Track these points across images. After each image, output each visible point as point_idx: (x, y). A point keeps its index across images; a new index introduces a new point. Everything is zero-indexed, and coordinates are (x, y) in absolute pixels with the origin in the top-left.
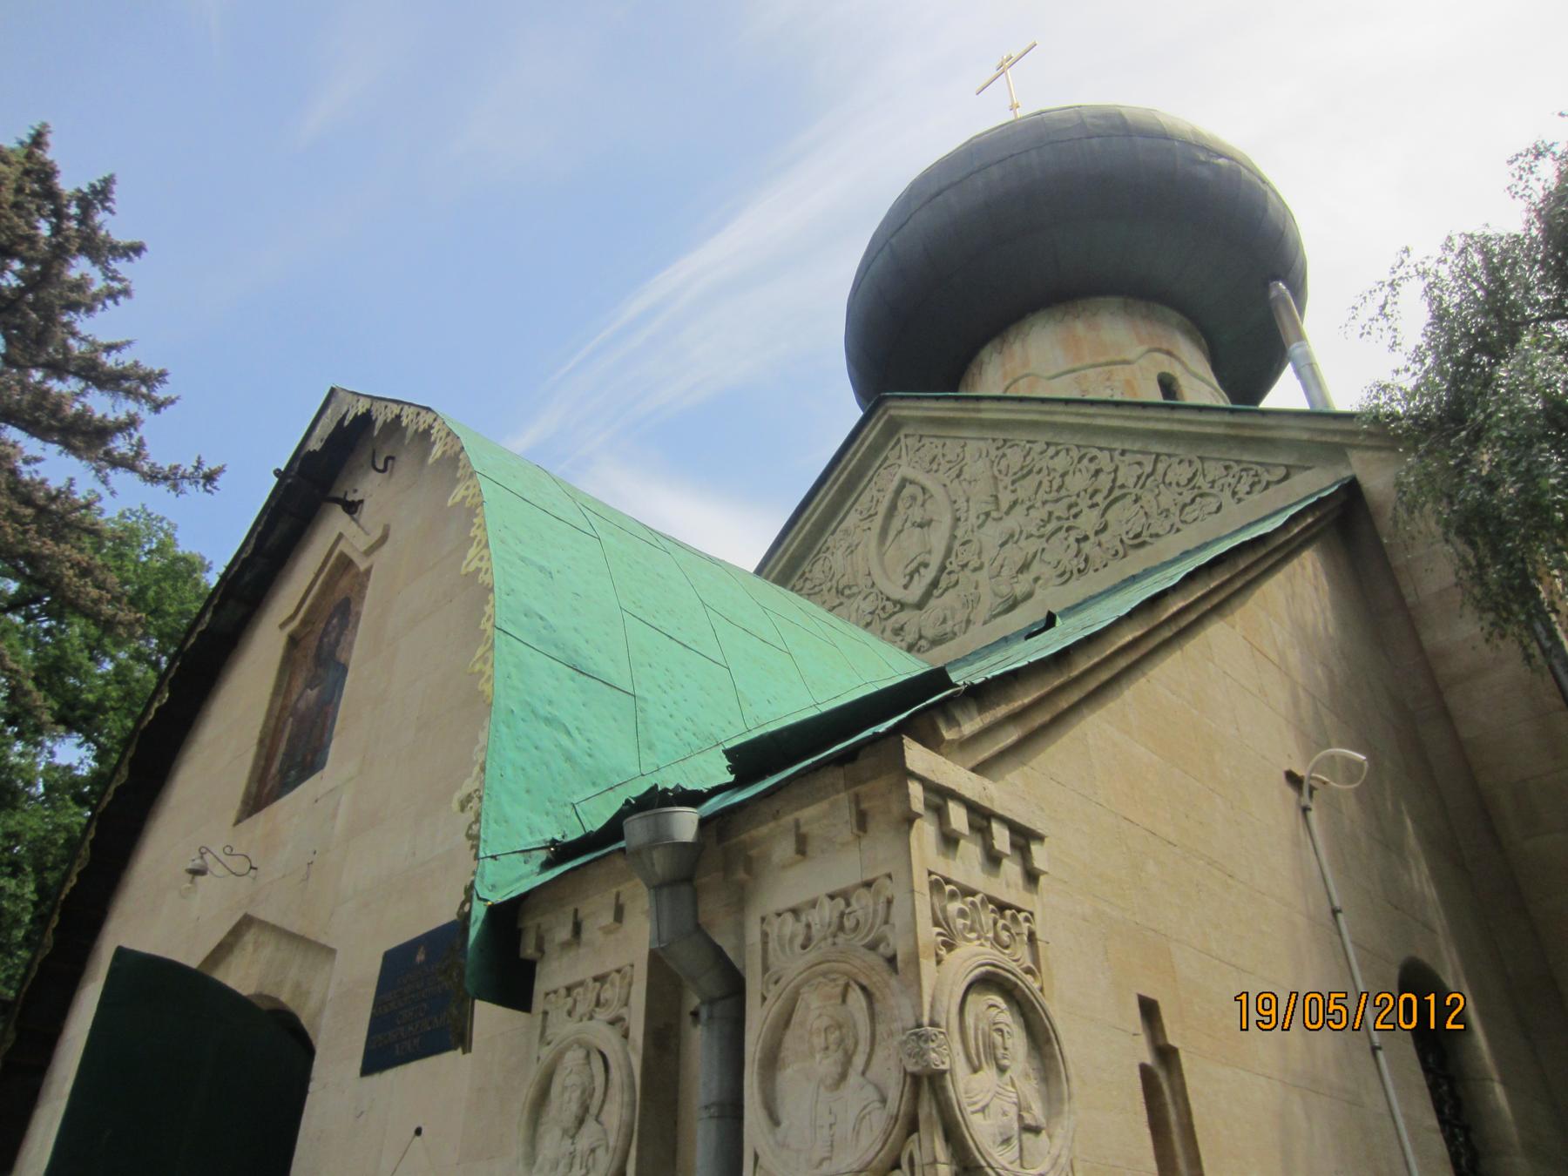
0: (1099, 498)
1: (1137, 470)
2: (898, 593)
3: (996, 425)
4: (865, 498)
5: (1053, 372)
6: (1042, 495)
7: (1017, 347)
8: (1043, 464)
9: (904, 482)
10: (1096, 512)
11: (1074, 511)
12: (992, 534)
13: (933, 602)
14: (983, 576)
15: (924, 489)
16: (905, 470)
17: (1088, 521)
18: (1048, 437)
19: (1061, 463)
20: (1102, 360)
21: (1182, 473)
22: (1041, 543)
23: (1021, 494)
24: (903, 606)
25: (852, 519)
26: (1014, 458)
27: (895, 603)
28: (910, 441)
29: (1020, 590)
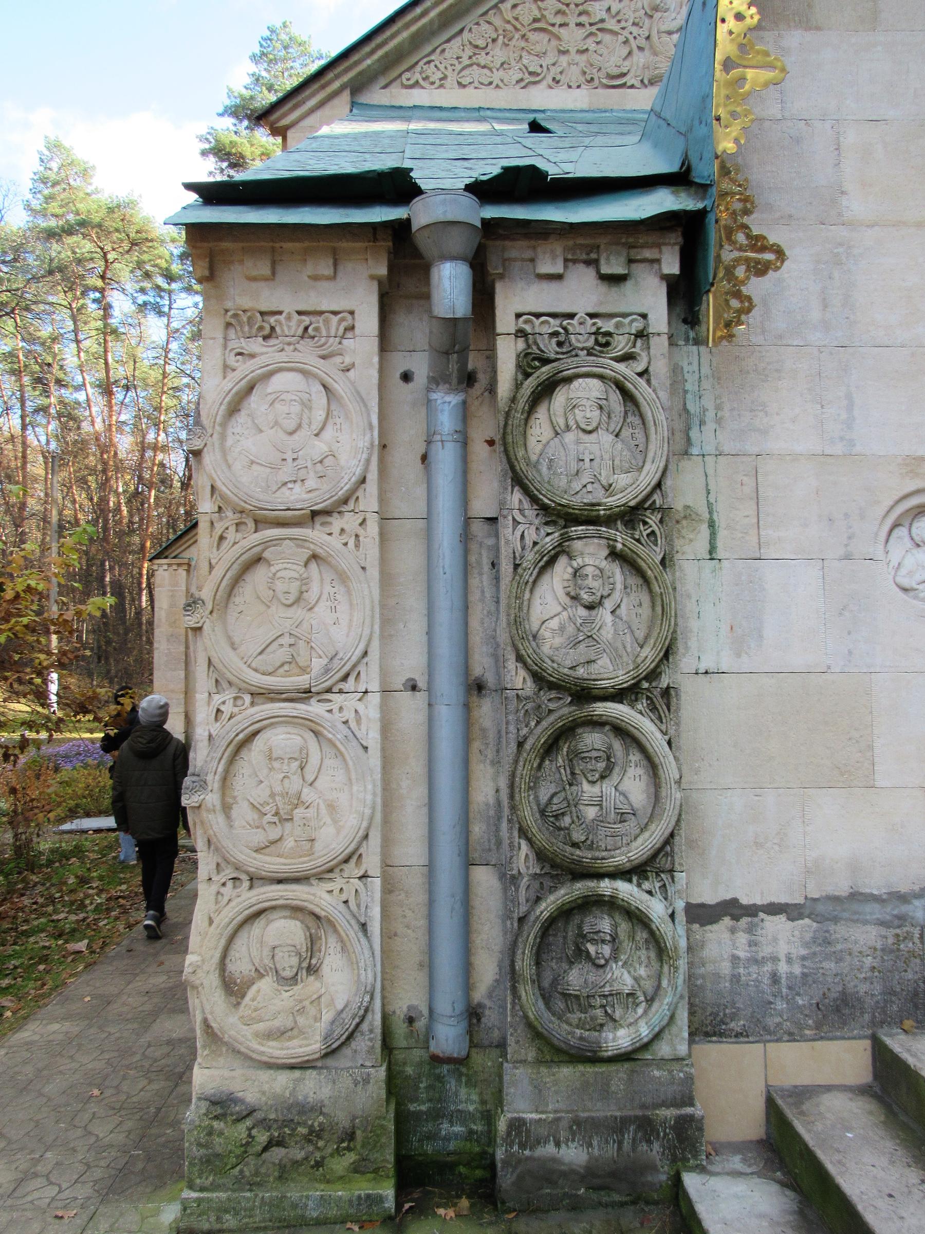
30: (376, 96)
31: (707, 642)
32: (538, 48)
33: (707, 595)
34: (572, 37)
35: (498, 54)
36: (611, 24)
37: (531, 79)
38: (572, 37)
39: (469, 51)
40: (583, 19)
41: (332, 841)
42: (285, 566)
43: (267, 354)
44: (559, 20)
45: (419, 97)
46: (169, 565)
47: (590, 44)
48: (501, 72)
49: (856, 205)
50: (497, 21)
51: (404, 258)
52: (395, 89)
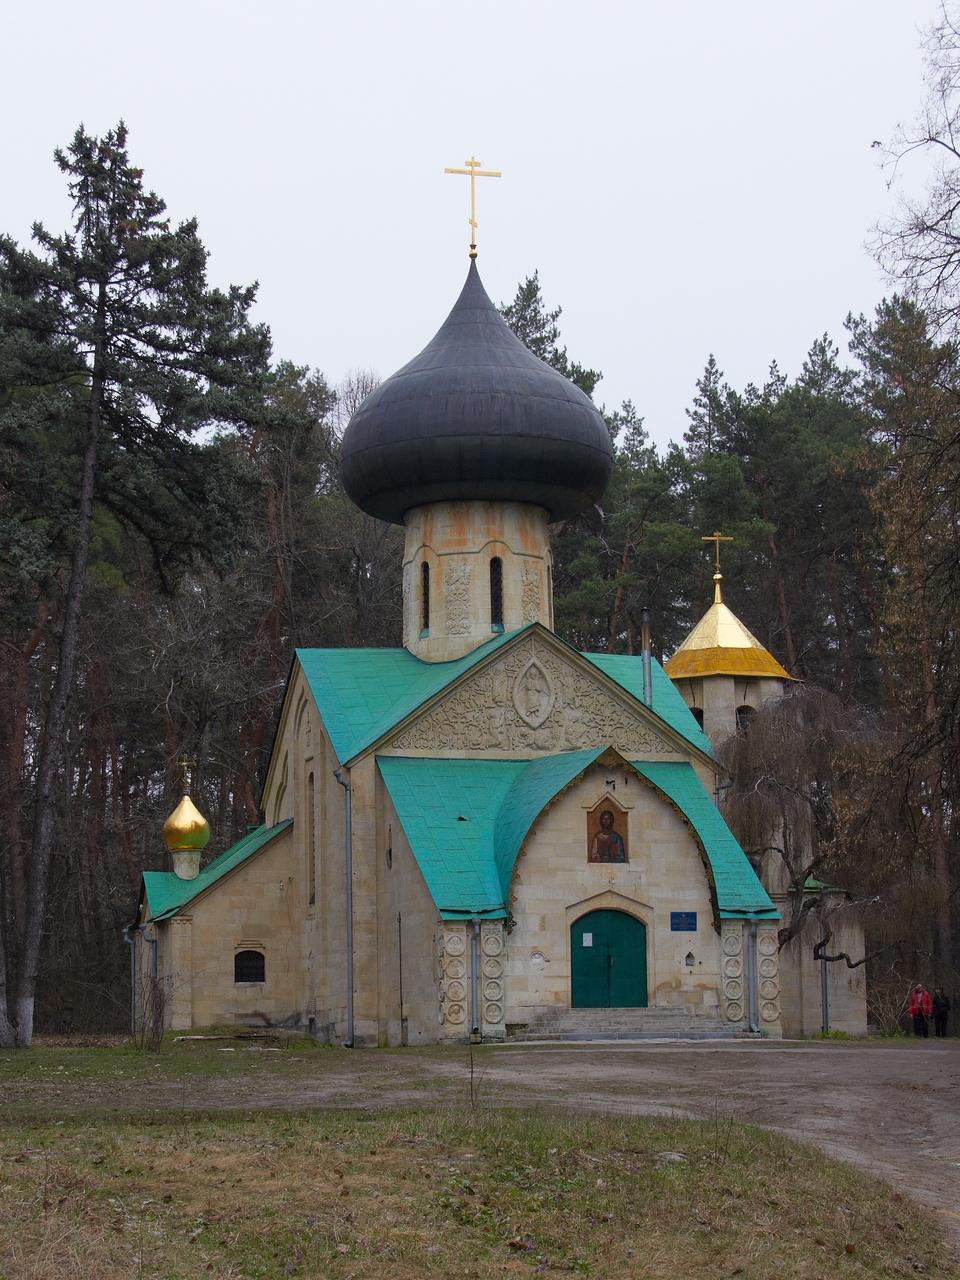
0: (612, 723)
1: (628, 720)
2: (528, 720)
3: (580, 666)
4: (511, 658)
5: (517, 551)
6: (591, 709)
7: (497, 516)
8: (595, 696)
9: (534, 665)
10: (610, 729)
11: (602, 723)
12: (568, 712)
13: (540, 730)
14: (563, 730)
15: (540, 672)
16: (534, 660)
17: (608, 730)
18: (597, 684)
19: (602, 699)
20: (536, 554)
21: (642, 731)
22: (586, 729)
23: (584, 704)
24: (527, 725)
25: (500, 666)
26: (584, 685)
27: (524, 722)
28: (537, 644)
29: (579, 745)
30: (384, 752)
31: (507, 972)
32: (446, 733)
33: (507, 966)
34: (459, 727)
35: (431, 735)
36: (474, 723)
37: (443, 745)
38: (459, 727)
39: (419, 733)
40: (463, 720)
41: (462, 996)
42: (456, 962)
43: (453, 934)
44: (454, 720)
45: (400, 753)
46: (181, 920)
47: (466, 731)
48: (431, 743)
49: (527, 911)
50: (430, 720)
51: (470, 924)
52: (390, 748)
